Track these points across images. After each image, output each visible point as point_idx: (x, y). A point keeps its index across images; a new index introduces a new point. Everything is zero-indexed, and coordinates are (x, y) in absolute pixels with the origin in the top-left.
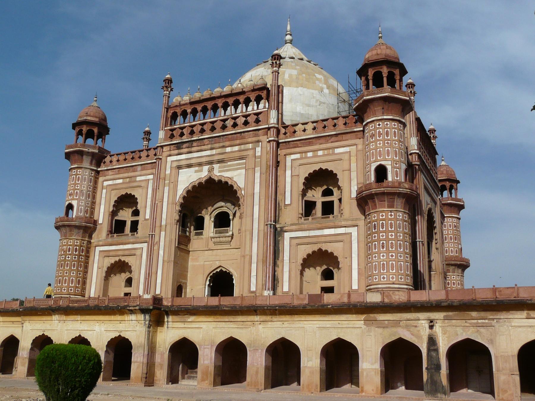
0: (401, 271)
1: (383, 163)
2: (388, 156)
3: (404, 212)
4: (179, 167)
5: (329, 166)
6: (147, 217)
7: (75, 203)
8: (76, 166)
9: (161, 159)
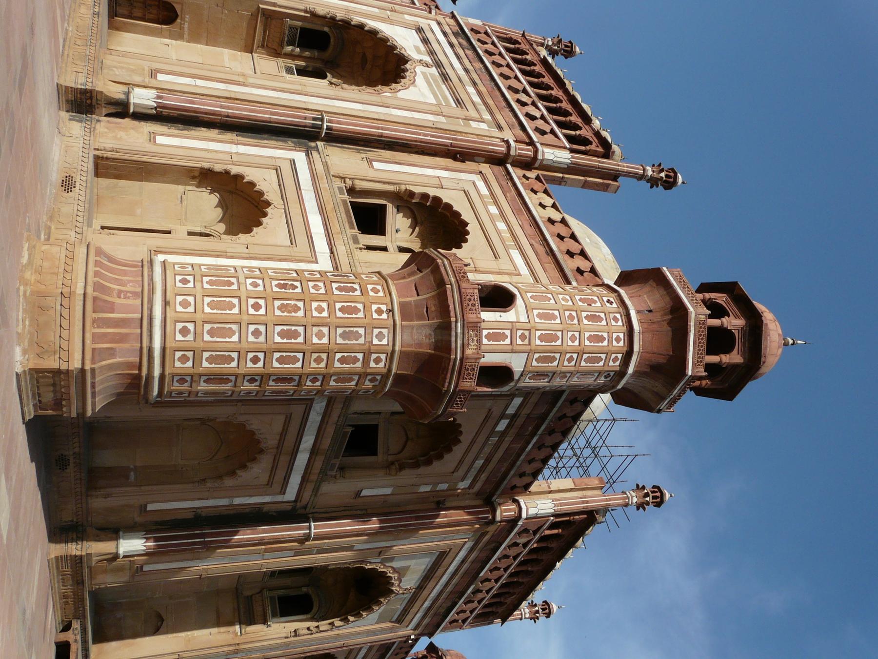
0: (211, 333)
1: (519, 301)
2: (539, 316)
3: (393, 351)
4: (419, 30)
9: (430, 12)
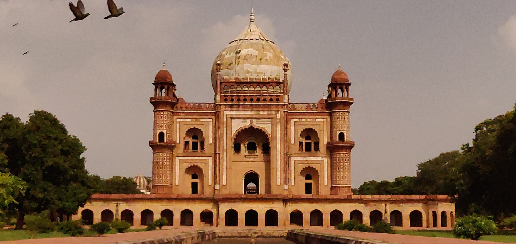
5: (314, 128)
6: (211, 142)
7: (165, 132)
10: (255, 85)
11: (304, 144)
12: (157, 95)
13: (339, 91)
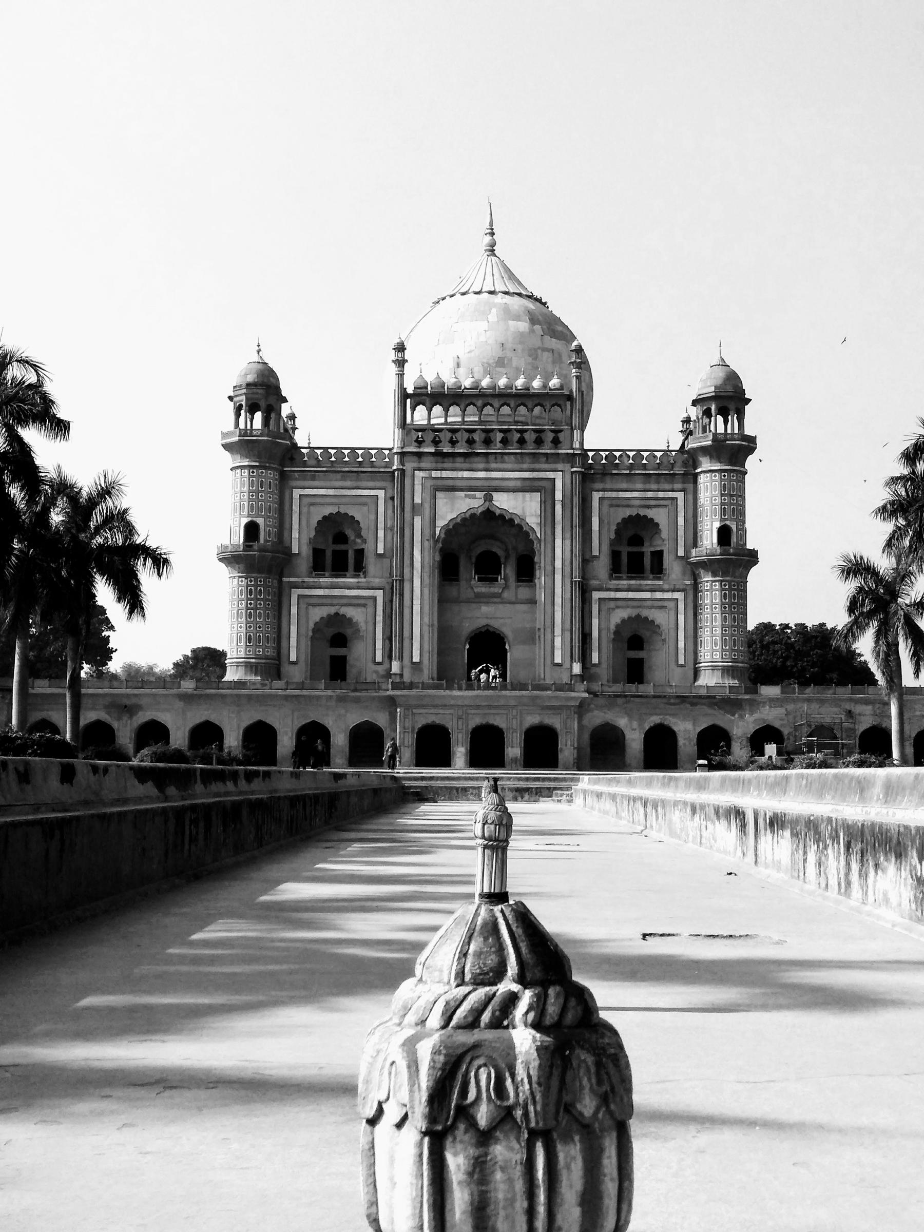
1: (728, 523)
4: (437, 489)
5: (650, 513)
6: (381, 550)
7: (260, 521)
8: (257, 464)
10: (496, 403)
11: (624, 559)
12: (242, 426)
13: (720, 419)
